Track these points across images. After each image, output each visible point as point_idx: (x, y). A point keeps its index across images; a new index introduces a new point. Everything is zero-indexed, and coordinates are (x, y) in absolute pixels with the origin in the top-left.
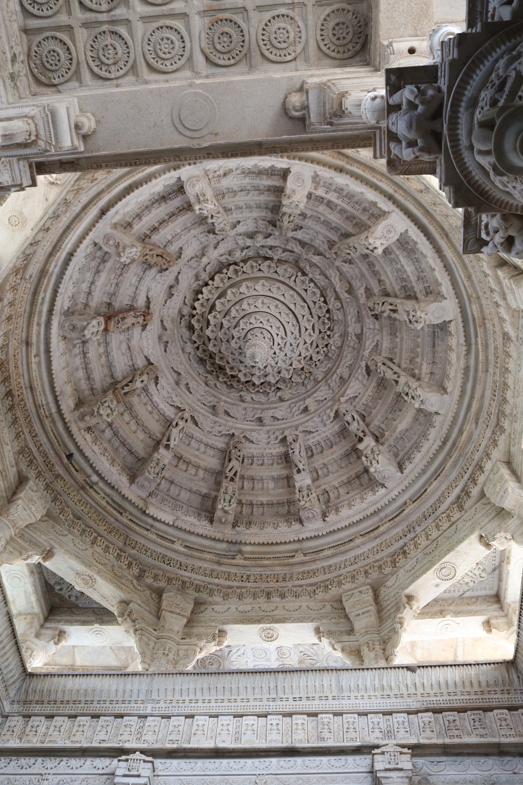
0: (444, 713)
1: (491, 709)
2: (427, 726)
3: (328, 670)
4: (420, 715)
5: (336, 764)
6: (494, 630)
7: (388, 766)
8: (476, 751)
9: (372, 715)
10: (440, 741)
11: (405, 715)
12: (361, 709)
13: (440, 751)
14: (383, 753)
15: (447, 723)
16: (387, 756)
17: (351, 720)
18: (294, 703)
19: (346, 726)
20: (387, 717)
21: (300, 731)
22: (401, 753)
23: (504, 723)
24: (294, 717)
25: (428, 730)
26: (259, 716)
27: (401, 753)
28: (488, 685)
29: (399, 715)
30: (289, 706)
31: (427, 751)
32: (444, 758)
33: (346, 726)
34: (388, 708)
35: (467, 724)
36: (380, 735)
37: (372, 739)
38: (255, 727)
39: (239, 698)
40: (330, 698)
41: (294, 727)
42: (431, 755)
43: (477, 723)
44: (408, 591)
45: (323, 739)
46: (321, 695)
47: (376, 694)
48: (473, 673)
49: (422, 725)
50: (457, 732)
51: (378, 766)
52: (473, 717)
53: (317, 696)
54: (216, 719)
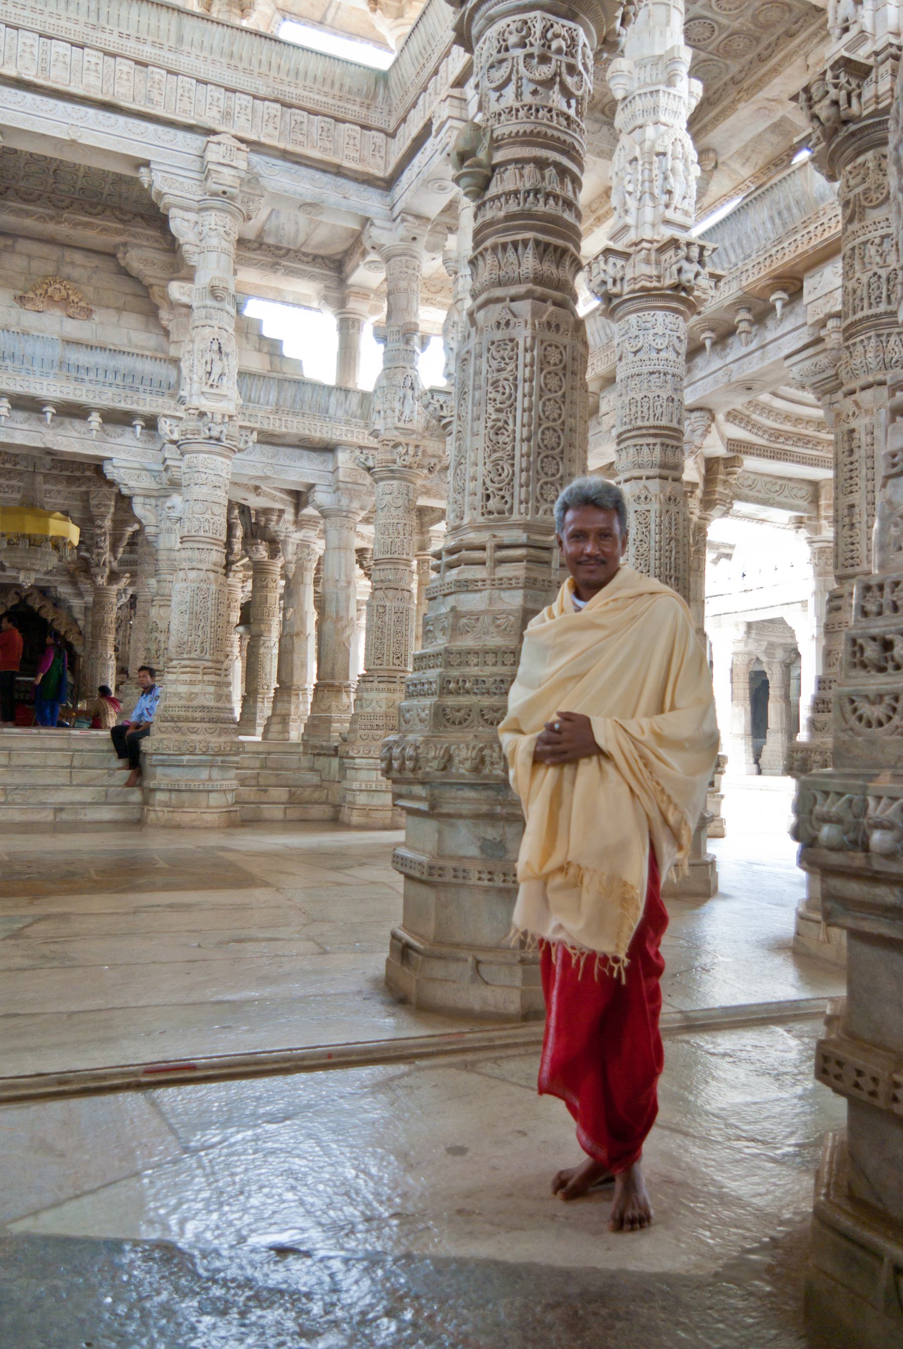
0: (293, 110)
1: (344, 122)
2: (271, 120)
3: (168, 7)
4: (267, 103)
5: (163, 137)
6: (379, 12)
7: (222, 161)
8: (315, 165)
9: (213, 87)
10: (281, 145)
11: (251, 98)
12: (202, 76)
13: (278, 154)
14: (219, 143)
15: (293, 123)
16: (222, 149)
17: (188, 86)
18: (119, 41)
19: (180, 91)
20: (230, 94)
21: (124, 83)
22: (238, 149)
23: (351, 142)
24: (119, 59)
25: (271, 126)
26: (73, 45)
27: (238, 149)
28: (350, 92)
29: (243, 96)
30: (113, 42)
31: (265, 150)
32: (280, 162)
33: (180, 91)
34: (232, 85)
35: (314, 130)
36: (218, 116)
37: (209, 119)
38: (68, 60)
39: (47, 10)
40: (166, 48)
41: (118, 74)
42: (268, 155)
43: (324, 134)
45: (151, 101)
46: (155, 40)
47: (222, 60)
48: (338, 71)
49: (266, 117)
50: (301, 138)
51: (210, 156)
52: (323, 124)
53: (150, 39)
54: (15, 31)
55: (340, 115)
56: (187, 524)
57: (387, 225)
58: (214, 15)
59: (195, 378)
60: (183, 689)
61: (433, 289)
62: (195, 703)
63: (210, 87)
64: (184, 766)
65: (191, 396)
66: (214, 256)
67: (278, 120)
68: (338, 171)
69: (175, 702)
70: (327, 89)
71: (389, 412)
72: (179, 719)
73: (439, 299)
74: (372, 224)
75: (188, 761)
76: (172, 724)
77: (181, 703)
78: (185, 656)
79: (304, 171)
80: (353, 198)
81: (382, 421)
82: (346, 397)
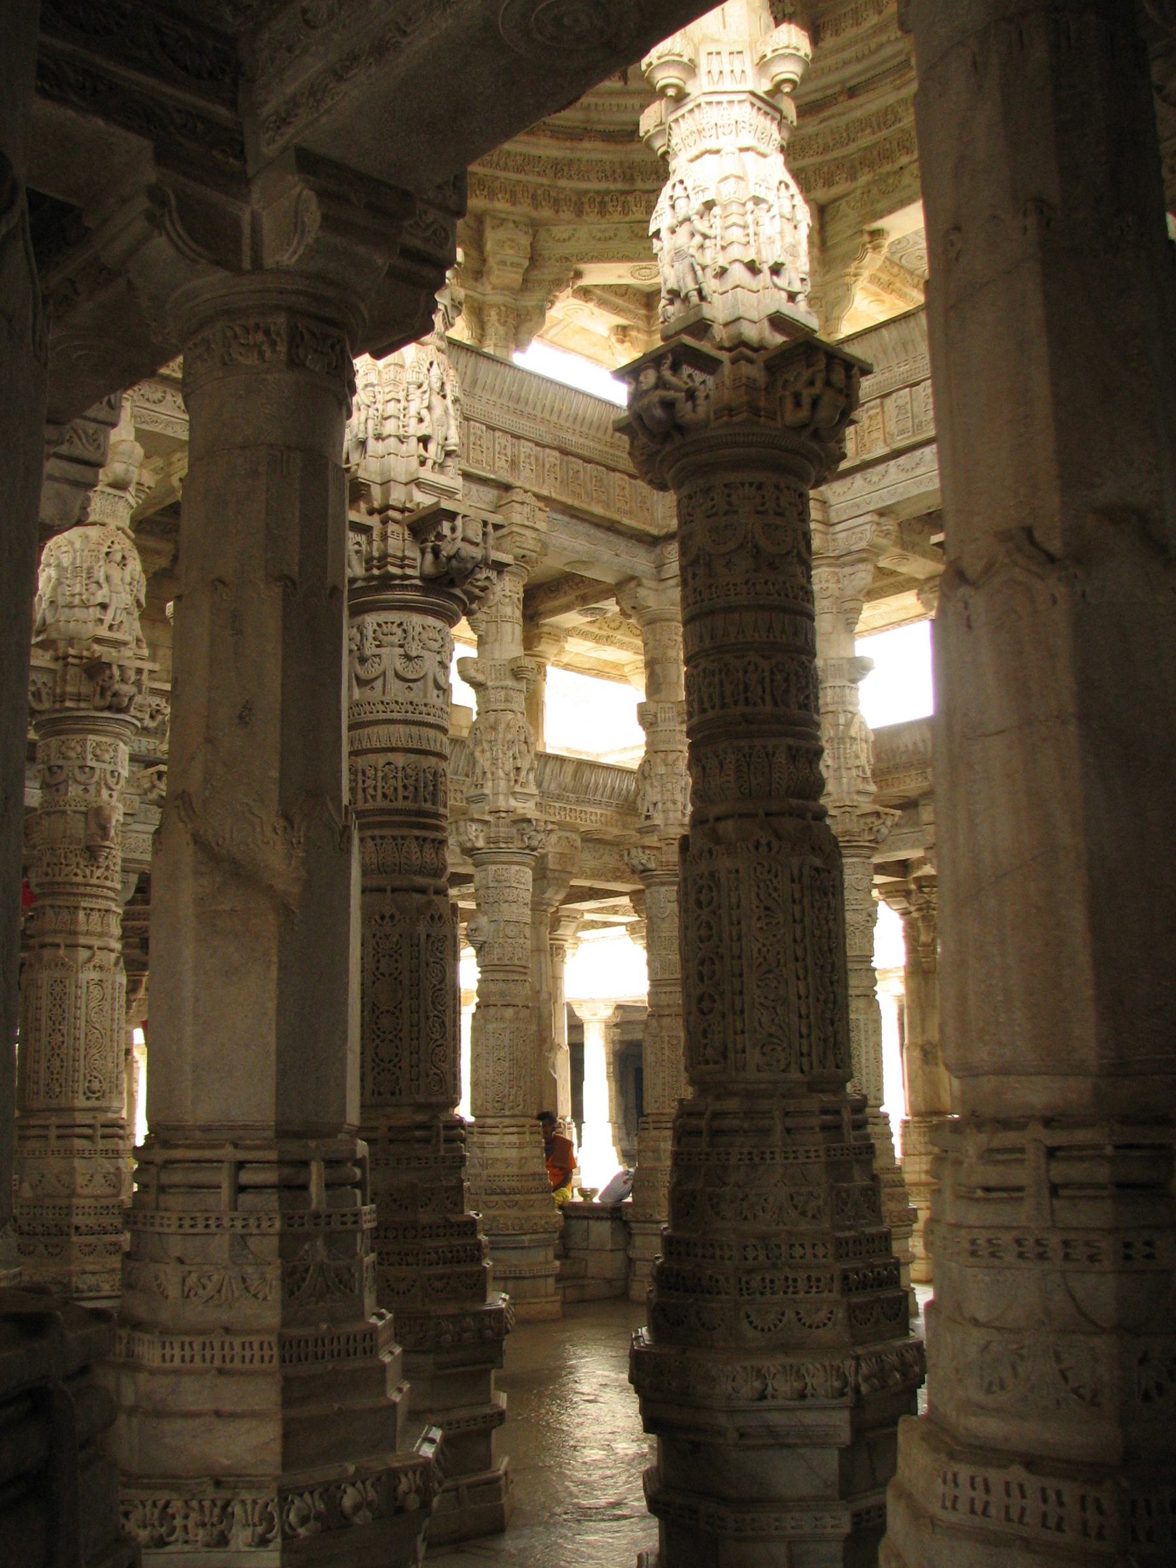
4: (548, 451)
7: (527, 523)
9: (500, 434)
16: (526, 509)
34: (520, 432)
36: (506, 466)
44: (582, 267)
55: (613, 464)
56: (497, 951)
57: (653, 584)
58: (489, 350)
59: (501, 773)
60: (512, 1153)
61: (613, 625)
62: (525, 1171)
63: (498, 434)
64: (523, 1248)
65: (496, 794)
66: (508, 626)
67: (558, 468)
68: (610, 527)
69: (500, 1169)
70: (600, 435)
71: (669, 805)
72: (514, 1191)
73: (619, 637)
74: (640, 585)
75: (530, 1240)
76: (504, 1198)
77: (510, 1171)
78: (507, 1113)
79: (581, 527)
80: (624, 555)
81: (661, 815)
82: (561, 767)
